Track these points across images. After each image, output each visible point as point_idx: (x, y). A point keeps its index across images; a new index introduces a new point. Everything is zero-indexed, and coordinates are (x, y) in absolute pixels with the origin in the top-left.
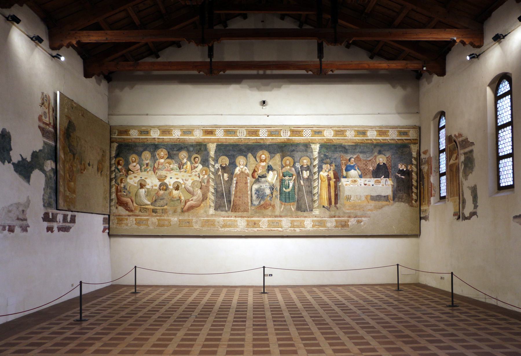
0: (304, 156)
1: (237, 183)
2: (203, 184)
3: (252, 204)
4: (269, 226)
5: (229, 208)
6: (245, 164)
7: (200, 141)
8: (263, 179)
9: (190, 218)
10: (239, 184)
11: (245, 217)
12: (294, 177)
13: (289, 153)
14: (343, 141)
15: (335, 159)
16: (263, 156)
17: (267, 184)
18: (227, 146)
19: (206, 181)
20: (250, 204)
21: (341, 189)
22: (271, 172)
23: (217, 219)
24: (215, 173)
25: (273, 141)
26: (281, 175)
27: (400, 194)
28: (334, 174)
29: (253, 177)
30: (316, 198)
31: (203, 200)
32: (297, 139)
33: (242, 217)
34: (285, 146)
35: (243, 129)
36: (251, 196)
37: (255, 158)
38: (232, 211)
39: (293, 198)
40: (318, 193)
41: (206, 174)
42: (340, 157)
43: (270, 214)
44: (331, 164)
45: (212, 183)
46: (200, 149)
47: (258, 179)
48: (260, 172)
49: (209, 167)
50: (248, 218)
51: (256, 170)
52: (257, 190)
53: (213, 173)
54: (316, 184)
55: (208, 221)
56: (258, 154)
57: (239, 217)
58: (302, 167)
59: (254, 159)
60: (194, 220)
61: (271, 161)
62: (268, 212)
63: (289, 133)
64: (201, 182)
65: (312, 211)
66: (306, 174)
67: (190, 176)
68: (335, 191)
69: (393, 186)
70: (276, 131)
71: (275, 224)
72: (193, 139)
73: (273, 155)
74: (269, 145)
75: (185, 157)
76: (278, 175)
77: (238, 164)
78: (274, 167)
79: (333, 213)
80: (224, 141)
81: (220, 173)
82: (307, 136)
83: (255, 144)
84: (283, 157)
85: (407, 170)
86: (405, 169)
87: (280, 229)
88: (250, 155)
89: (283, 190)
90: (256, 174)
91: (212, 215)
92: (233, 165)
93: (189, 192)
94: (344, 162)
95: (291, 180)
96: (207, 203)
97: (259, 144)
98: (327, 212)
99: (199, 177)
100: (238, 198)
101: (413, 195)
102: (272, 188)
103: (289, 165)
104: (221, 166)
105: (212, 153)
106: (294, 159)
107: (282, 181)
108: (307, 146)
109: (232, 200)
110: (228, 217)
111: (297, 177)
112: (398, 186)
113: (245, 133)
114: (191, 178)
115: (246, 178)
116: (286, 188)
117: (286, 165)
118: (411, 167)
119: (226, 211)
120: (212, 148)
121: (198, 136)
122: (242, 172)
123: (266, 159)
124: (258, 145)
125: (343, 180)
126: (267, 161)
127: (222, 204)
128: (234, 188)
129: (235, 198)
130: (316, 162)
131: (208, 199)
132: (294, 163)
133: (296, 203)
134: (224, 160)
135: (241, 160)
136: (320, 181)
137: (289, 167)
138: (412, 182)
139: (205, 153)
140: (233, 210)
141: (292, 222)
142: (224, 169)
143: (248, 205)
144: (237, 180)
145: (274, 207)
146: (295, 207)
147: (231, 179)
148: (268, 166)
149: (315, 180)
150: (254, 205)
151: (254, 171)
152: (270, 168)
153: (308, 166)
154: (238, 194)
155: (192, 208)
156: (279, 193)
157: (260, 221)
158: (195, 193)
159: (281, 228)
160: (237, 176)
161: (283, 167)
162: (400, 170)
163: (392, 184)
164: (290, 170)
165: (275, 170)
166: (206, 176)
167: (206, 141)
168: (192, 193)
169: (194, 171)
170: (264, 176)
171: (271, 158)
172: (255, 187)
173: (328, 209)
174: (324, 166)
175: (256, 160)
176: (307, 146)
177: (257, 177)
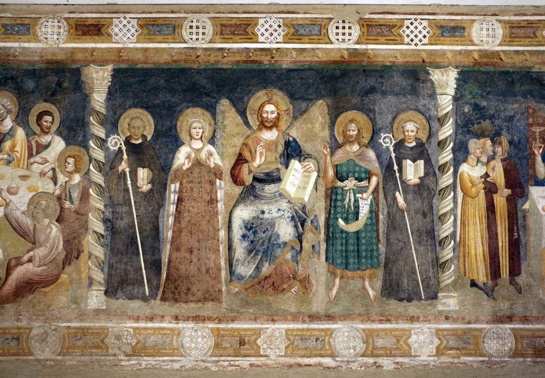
0: (408, 109)
1: (180, 200)
2: (67, 204)
3: (231, 272)
4: (291, 349)
5: (154, 288)
6: (208, 134)
7: (60, 57)
8: (270, 189)
9: (24, 323)
10: (186, 204)
11: (210, 319)
12: (374, 180)
13: (356, 100)
14: (534, 59)
15: (510, 119)
16: (270, 108)
17: (284, 205)
18: (148, 73)
19: (76, 195)
20: (224, 274)
21: (531, 222)
22: (295, 164)
23: (114, 326)
24: (109, 167)
25: (301, 58)
26: (331, 172)
28: (507, 172)
29: (236, 179)
30: (447, 253)
31: (67, 261)
32: (381, 50)
33: (196, 319)
34: (345, 73)
35: (204, 17)
36: (230, 248)
37: (243, 114)
38: (164, 299)
39: (372, 254)
40: (453, 235)
41: (77, 170)
42: (526, 113)
43: (293, 310)
44: (495, 139)
45: (97, 202)
46: (59, 84)
47: (252, 187)
48: (259, 162)
49: (86, 147)
50: (220, 321)
51: (247, 155)
52: (250, 227)
53: (100, 167)
54: (446, 205)
55: (84, 331)
56: (254, 102)
57: (187, 319)
58: (399, 145)
59: (239, 119)
60: (34, 332)
61: (297, 124)
62: (288, 301)
63: (356, 32)
64: (59, 198)
65: (435, 297)
66: (413, 171)
67: (24, 177)
68: (511, 232)
70: (313, 23)
71: (312, 343)
72: (34, 51)
73: (304, 105)
74: (289, 71)
75: (9, 112)
76: (321, 173)
77: (183, 136)
78: (306, 147)
79: (504, 306)
80: (140, 56)
81: (124, 166)
82: (416, 41)
83: (243, 66)
84: (335, 114)
87: (328, 361)
88: (224, 104)
89: (336, 225)
90: (245, 168)
91: (97, 312)
92: (169, 138)
93: (21, 232)
94: (537, 130)
95: (362, 190)
96: (79, 272)
97: (255, 66)
98: (487, 305)
99: (54, 179)
100: (184, 254)
102: (300, 219)
103: (358, 139)
104: (127, 142)
105: (99, 99)
106: (373, 121)
107: (333, 196)
108: (416, 75)
109: (165, 259)
110: (151, 319)
111: (385, 179)
113: (209, 30)
114: (29, 183)
115: (212, 183)
116: (346, 220)
117: (348, 141)
119: (145, 299)
120: (99, 82)
121: (52, 40)
122: (198, 163)
123: (278, 118)
124: (254, 70)
125: (535, 191)
126: (283, 125)
127: (132, 275)
128: (171, 220)
129: (175, 255)
130: (447, 131)
131: (84, 256)
132: (375, 133)
133: (380, 273)
134: (137, 123)
135: (194, 122)
136: (460, 195)
137: (356, 147)
139: (77, 96)
140: (169, 295)
141: (369, 337)
142: (137, 152)
143: (217, 278)
144: (180, 191)
145: (305, 283)
146: (379, 284)
147: (160, 186)
148: (287, 144)
149: (443, 192)
150: (241, 278)
151: (240, 160)
152: (292, 151)
153: (420, 145)
154: (185, 238)
155: (29, 286)
156: (322, 236)
157: (258, 333)
158: (41, 237)
159: (333, 356)
160: (181, 175)
161: (335, 146)
164: (361, 155)
165: (309, 156)
166: (77, 178)
167: (79, 56)
168: (30, 238)
169: (38, 159)
170: (273, 178)
171: (298, 114)
172: (243, 213)
173: (489, 292)
174: (475, 145)
175: (247, 123)
176: (416, 75)
177: (248, 180)
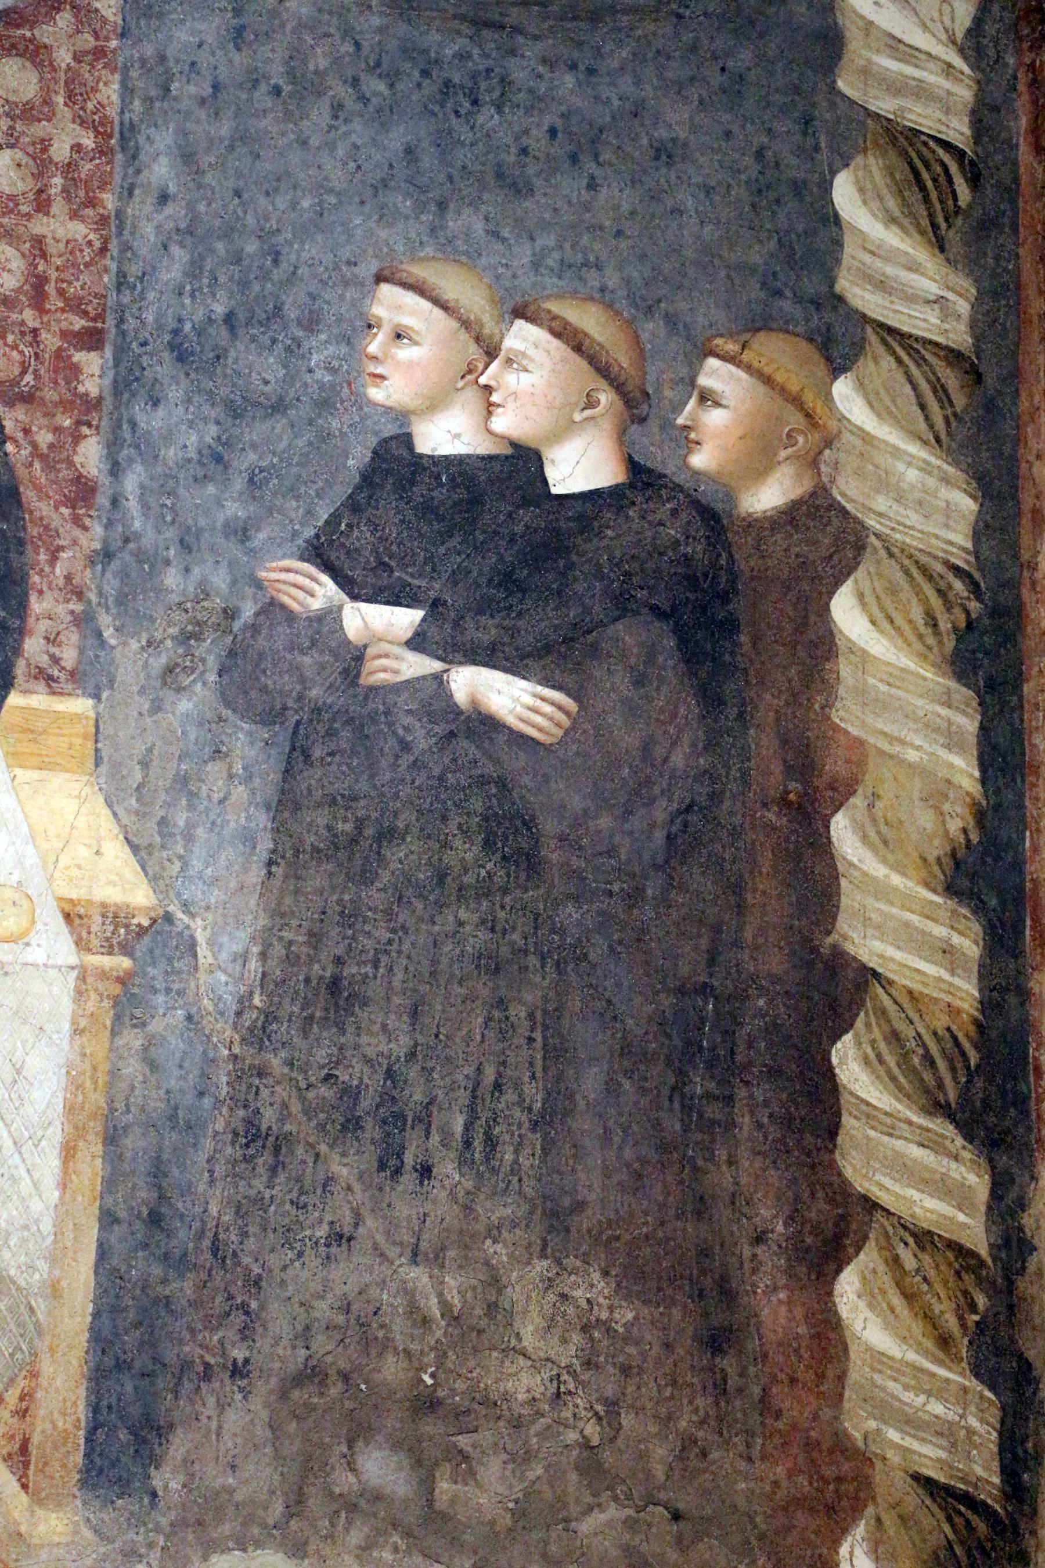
27: (376, 1261)
69: (133, 960)
85: (642, 478)
86: (580, 466)
101: (864, 1308)
112: (316, 989)
118: (803, 427)
138: (815, 883)
162: (395, 463)
163: (121, 883)
